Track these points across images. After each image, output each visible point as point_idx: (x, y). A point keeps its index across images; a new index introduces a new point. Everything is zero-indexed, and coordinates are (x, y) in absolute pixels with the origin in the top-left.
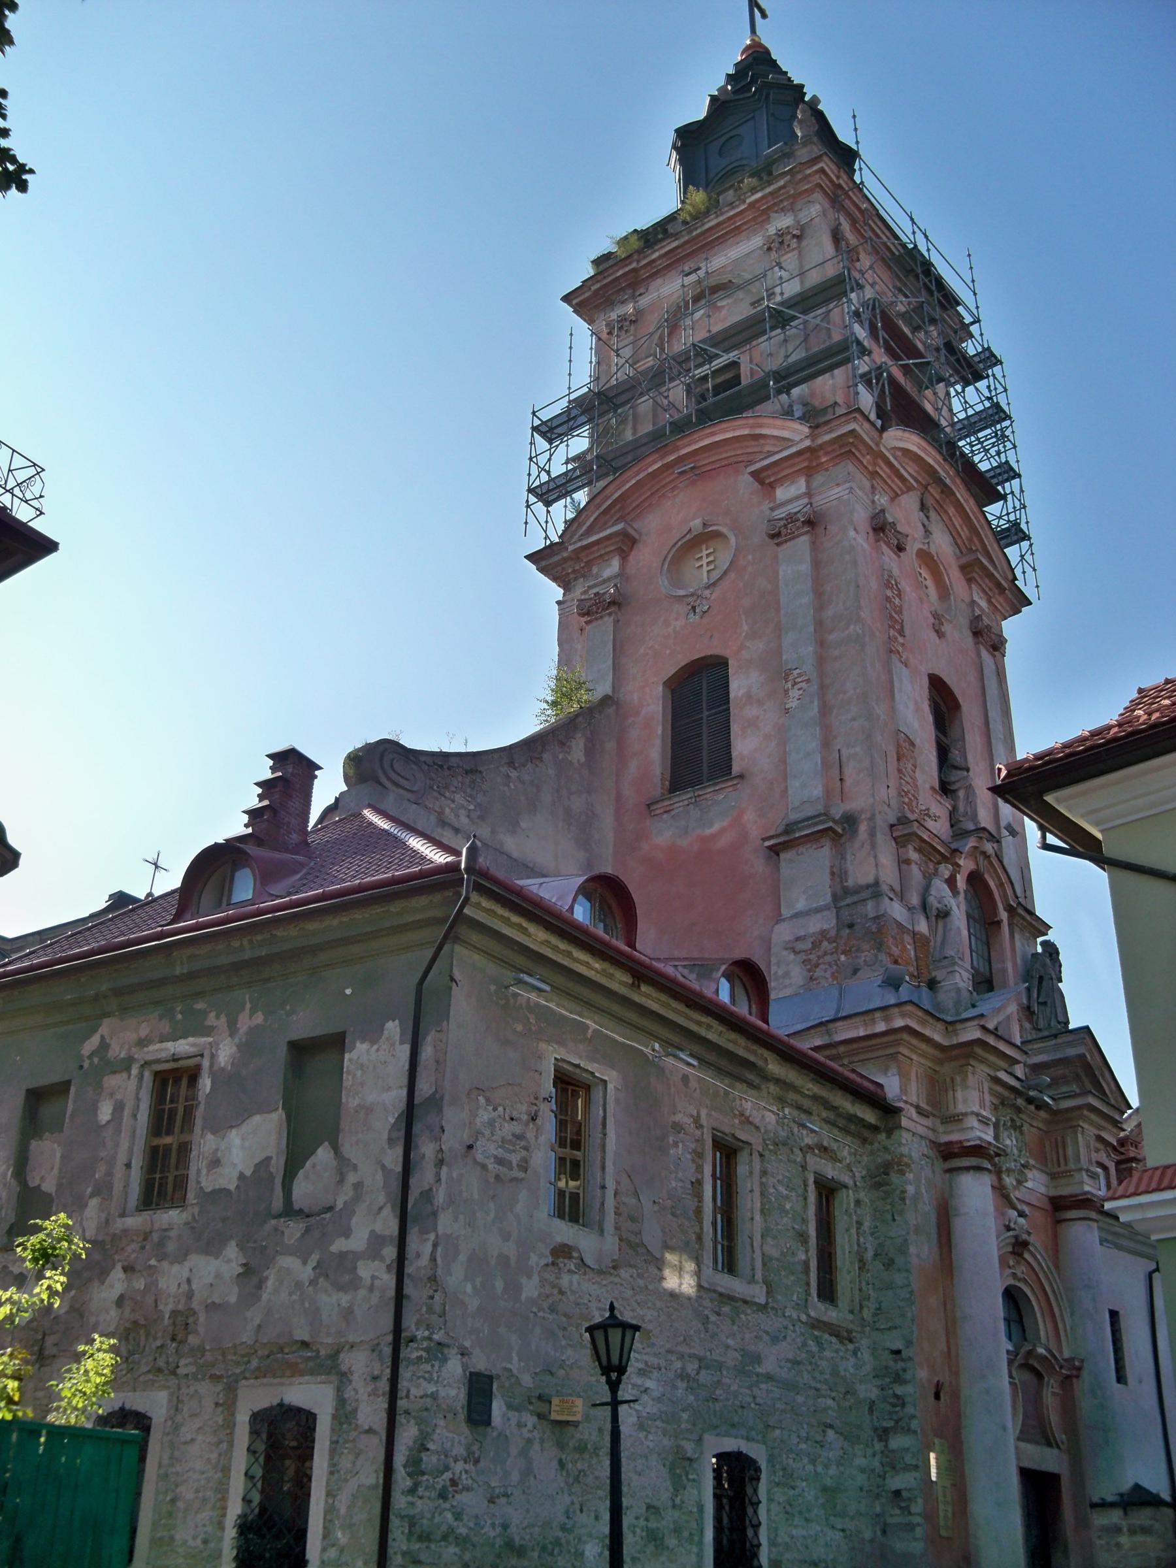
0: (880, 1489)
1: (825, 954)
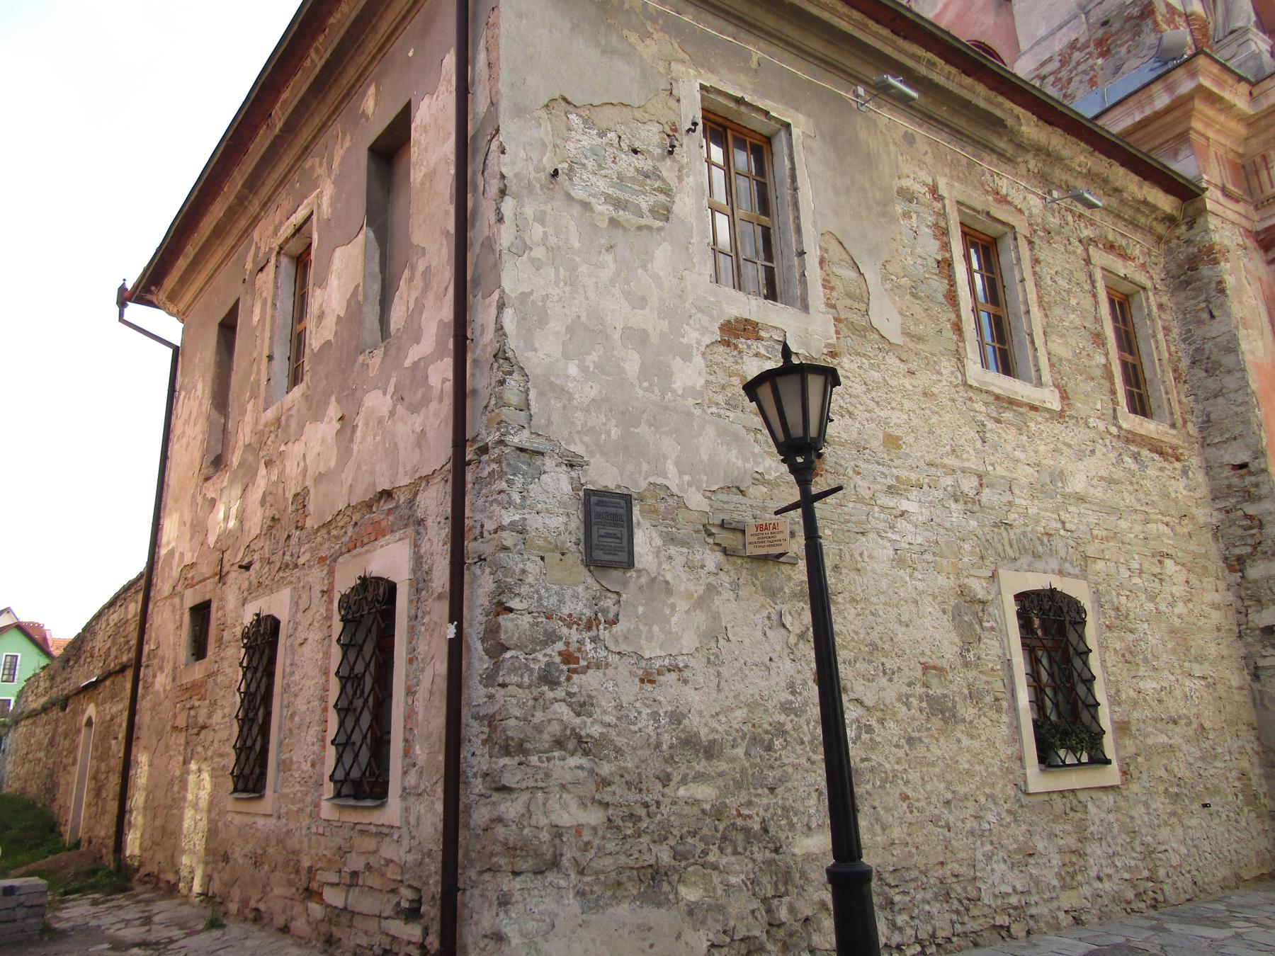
0: (1244, 627)
1: (1078, 64)
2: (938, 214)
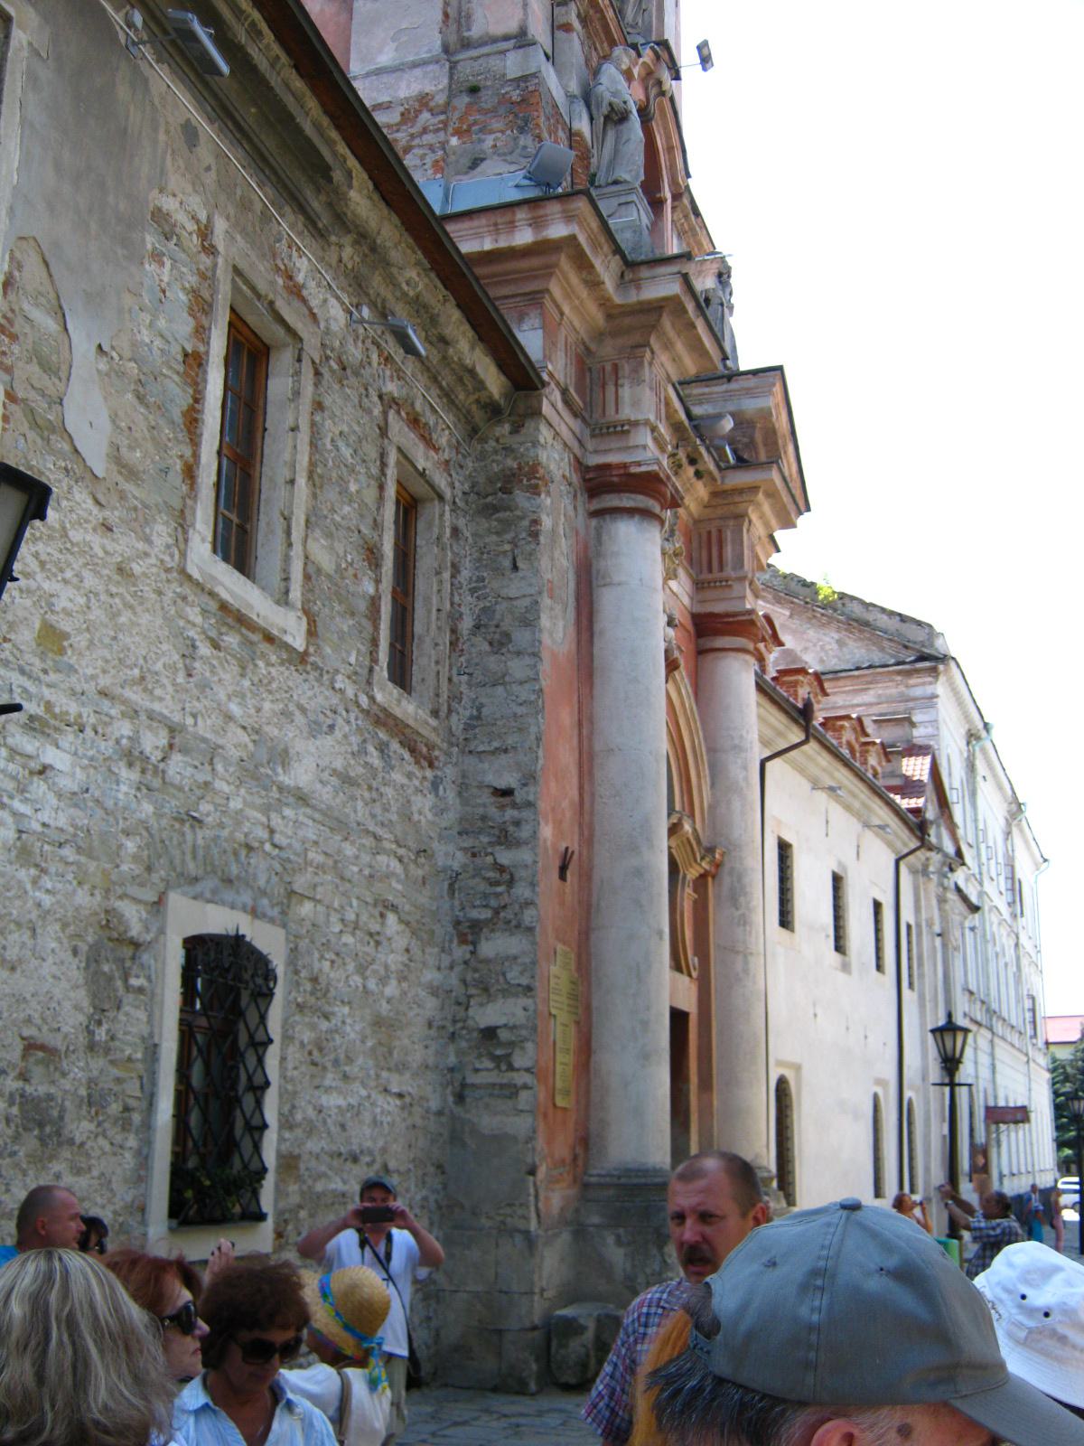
0: (459, 1025)
1: (425, 131)
2: (202, 276)
